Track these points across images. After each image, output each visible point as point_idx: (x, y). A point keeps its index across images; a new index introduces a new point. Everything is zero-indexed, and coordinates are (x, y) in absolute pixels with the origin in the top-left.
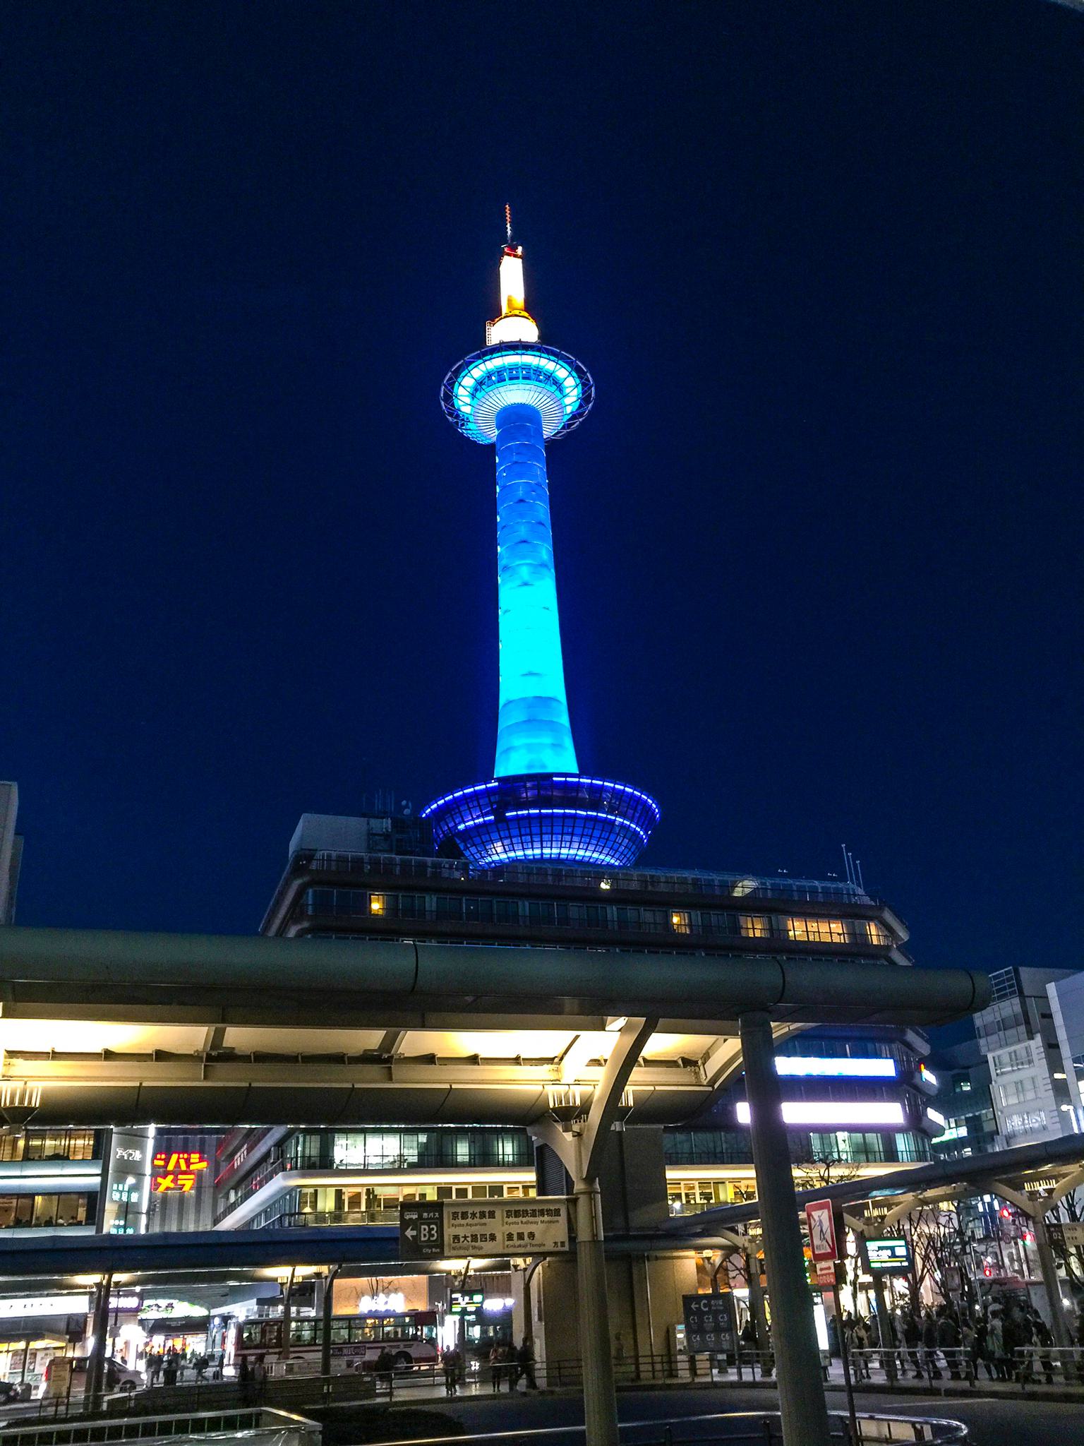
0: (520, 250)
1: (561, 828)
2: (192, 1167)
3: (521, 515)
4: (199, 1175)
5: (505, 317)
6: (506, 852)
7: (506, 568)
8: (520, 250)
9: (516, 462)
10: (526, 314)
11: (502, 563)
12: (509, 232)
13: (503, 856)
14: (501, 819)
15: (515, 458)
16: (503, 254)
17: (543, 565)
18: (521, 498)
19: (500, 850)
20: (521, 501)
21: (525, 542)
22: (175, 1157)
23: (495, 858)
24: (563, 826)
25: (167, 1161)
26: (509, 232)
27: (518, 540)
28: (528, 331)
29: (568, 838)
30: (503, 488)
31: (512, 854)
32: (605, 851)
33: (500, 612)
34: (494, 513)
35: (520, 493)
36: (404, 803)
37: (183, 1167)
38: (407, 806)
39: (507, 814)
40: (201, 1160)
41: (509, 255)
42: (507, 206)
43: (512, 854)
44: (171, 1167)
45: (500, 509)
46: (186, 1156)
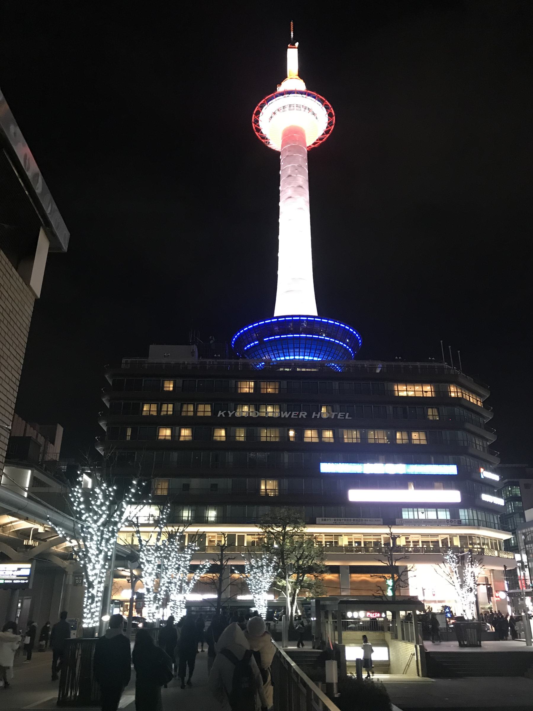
0: (297, 44)
1: (293, 345)
3: (289, 184)
8: (297, 44)
9: (288, 156)
10: (298, 77)
12: (292, 36)
14: (262, 342)
15: (287, 154)
16: (288, 48)
20: (290, 176)
21: (290, 197)
24: (294, 344)
26: (292, 36)
28: (301, 85)
29: (297, 350)
35: (289, 172)
36: (210, 337)
38: (211, 339)
39: (265, 340)
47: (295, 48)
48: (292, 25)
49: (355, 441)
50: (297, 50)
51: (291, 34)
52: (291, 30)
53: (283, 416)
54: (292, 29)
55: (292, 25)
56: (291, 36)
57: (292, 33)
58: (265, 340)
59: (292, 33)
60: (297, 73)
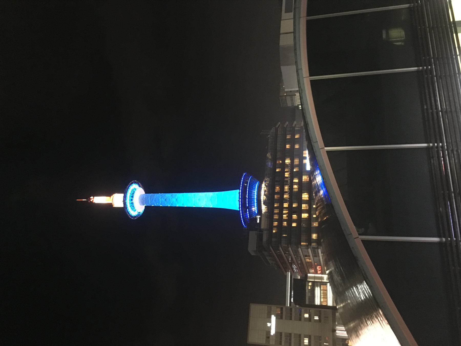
3: (170, 200)
5: (113, 202)
6: (255, 207)
9: (155, 201)
10: (112, 196)
13: (256, 208)
17: (194, 195)
18: (165, 200)
19: (254, 208)
20: (166, 200)
23: (256, 209)
27: (176, 201)
30: (161, 204)
31: (256, 206)
32: (255, 185)
34: (167, 207)
39: (247, 206)
41: (93, 200)
42: (77, 200)
43: (256, 206)
45: (166, 205)
47: (93, 198)
48: (78, 200)
49: (298, 161)
50: (95, 197)
51: (84, 201)
52: (81, 201)
53: (289, 182)
54: (81, 200)
55: (78, 200)
56: (85, 201)
57: (83, 200)
58: (247, 206)
59: (83, 200)
60: (109, 198)
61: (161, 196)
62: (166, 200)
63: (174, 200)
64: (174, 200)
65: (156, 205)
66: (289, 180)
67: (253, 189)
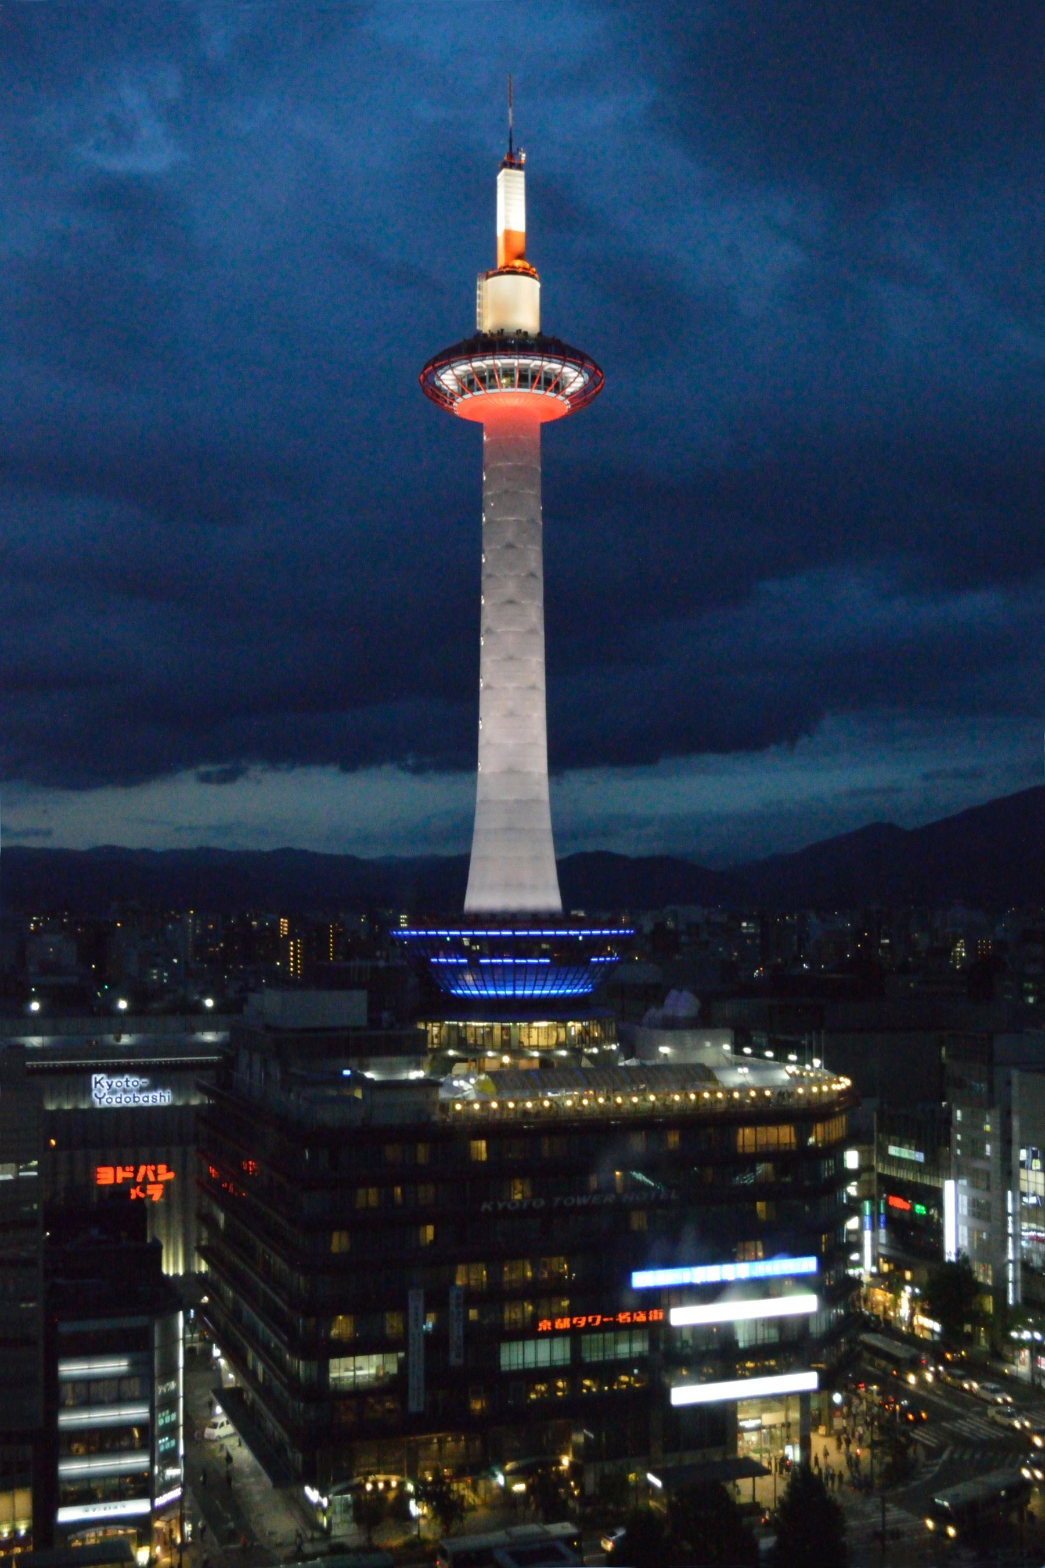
2: (160, 1178)
4: (167, 1184)
7: (489, 576)
9: (506, 492)
11: (486, 571)
20: (510, 546)
22: (142, 1169)
25: (136, 1172)
33: (483, 578)
34: (480, 551)
35: (509, 536)
37: (152, 1178)
40: (168, 1170)
44: (139, 1179)
45: (486, 547)
46: (153, 1167)
61: (533, 521)
62: (510, 546)
63: (510, 588)
64: (510, 588)
65: (488, 493)
66: (591, 1201)
67: (560, 982)
